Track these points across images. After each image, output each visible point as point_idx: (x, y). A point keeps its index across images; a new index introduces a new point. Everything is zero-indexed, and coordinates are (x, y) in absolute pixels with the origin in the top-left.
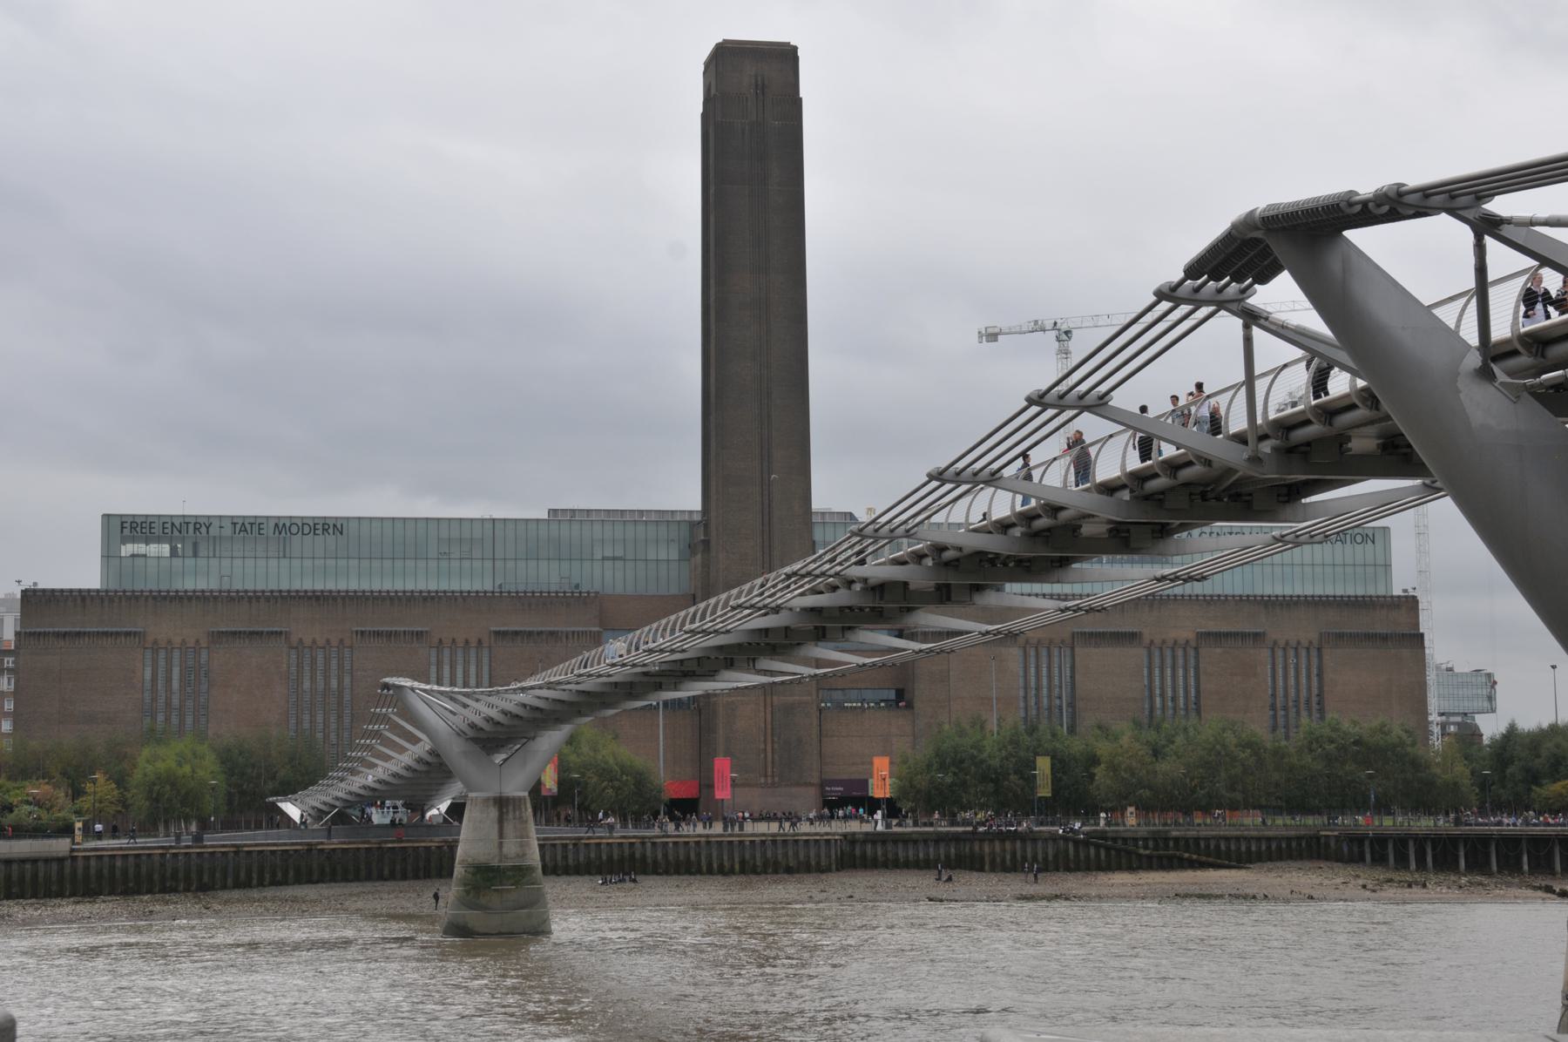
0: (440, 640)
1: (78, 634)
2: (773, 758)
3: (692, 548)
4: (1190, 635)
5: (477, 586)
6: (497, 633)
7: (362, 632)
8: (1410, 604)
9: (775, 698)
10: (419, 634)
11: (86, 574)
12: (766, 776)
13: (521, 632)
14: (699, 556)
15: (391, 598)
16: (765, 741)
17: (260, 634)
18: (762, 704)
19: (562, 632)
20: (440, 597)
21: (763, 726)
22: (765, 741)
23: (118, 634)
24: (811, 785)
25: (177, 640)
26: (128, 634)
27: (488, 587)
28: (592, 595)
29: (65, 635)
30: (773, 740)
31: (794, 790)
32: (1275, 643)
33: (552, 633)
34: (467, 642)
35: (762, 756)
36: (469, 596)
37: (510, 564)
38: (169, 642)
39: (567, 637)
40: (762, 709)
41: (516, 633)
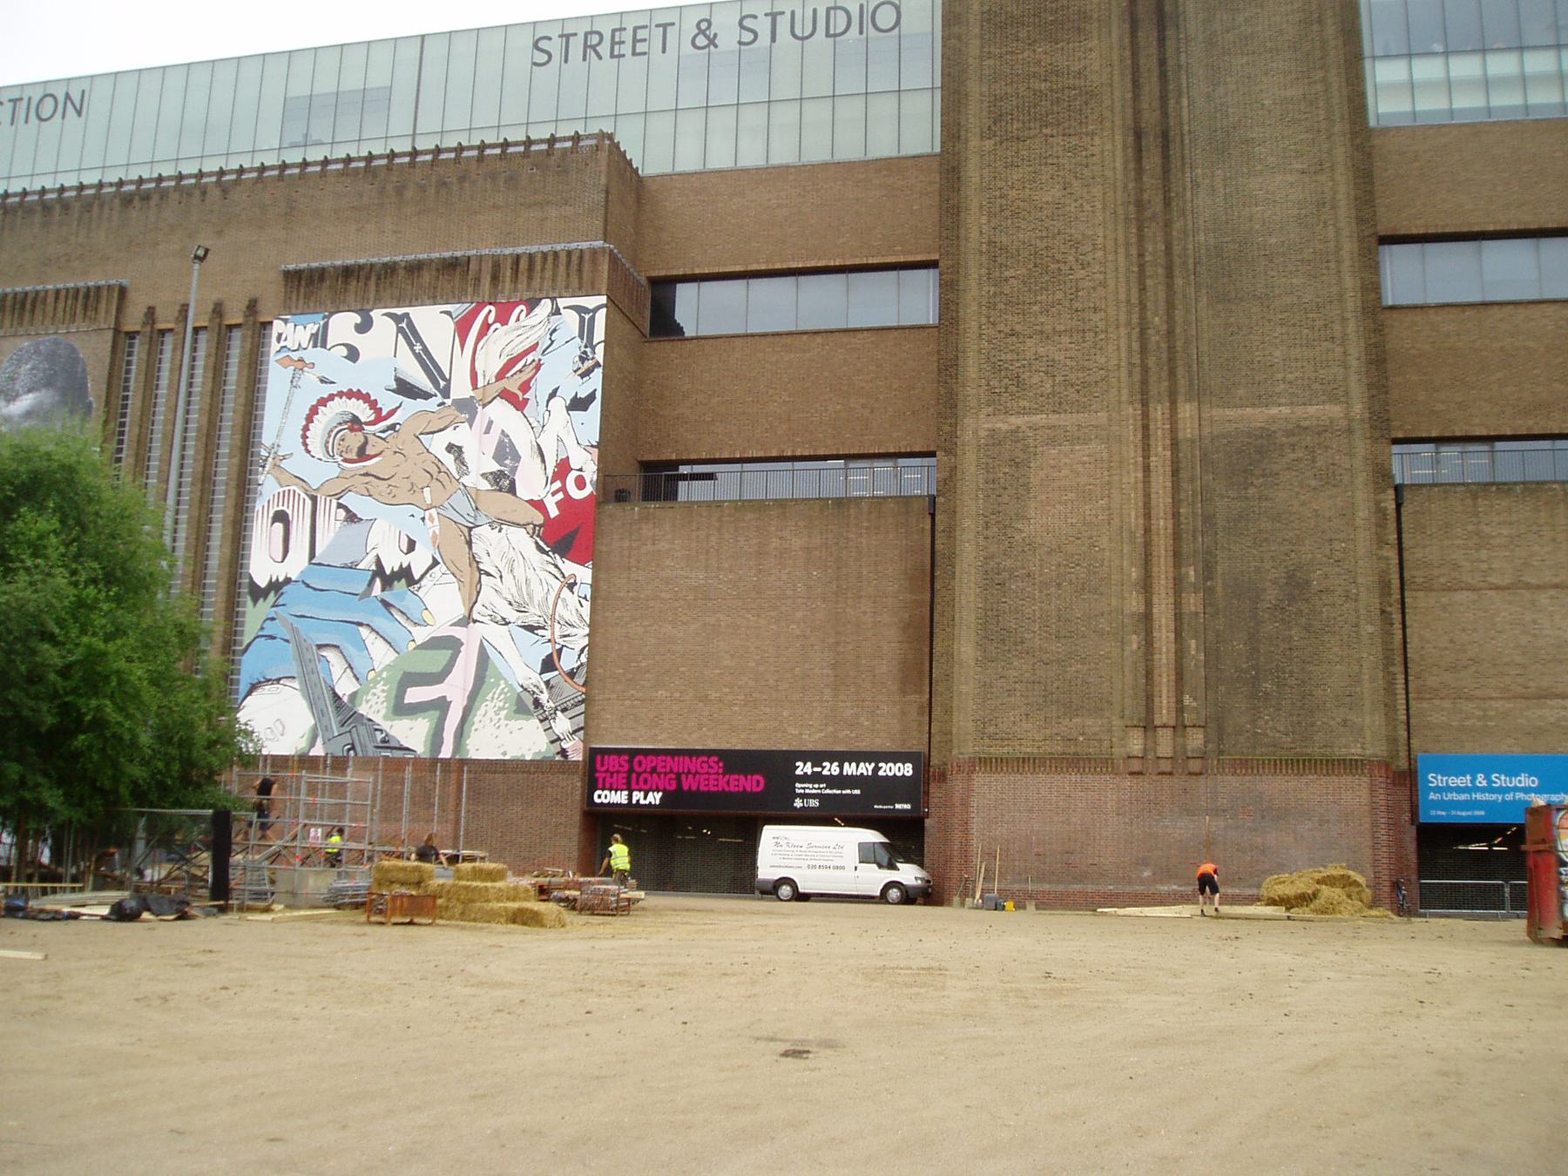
0: (151, 313)
2: (1180, 653)
9: (1186, 410)
12: (1148, 727)
13: (361, 267)
15: (46, 207)
16: (1146, 586)
18: (1132, 434)
19: (480, 258)
20: (164, 194)
21: (1134, 519)
22: (1146, 586)
24: (1352, 766)
30: (1178, 584)
31: (1277, 786)
33: (452, 266)
35: (1134, 642)
36: (237, 182)
39: (495, 278)
40: (1133, 454)
41: (348, 273)
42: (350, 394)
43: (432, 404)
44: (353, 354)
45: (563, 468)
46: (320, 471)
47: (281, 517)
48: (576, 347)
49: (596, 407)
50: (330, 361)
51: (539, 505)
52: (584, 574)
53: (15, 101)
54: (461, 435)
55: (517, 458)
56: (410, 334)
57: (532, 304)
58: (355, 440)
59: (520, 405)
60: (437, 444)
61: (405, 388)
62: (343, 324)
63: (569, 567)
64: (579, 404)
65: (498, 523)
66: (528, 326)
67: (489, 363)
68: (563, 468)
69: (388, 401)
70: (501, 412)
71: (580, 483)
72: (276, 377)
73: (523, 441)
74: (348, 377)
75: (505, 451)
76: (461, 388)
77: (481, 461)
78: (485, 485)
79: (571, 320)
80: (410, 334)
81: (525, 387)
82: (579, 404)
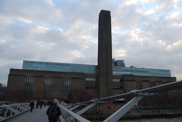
1: (17, 75)
3: (97, 69)
4: (154, 81)
5: (70, 72)
6: (72, 78)
10: (62, 77)
11: (20, 67)
14: (98, 69)
17: (40, 76)
23: (21, 75)
25: (30, 76)
26: (23, 75)
27: (71, 72)
29: (15, 75)
33: (79, 78)
37: (74, 69)
38: (29, 77)
41: (74, 78)
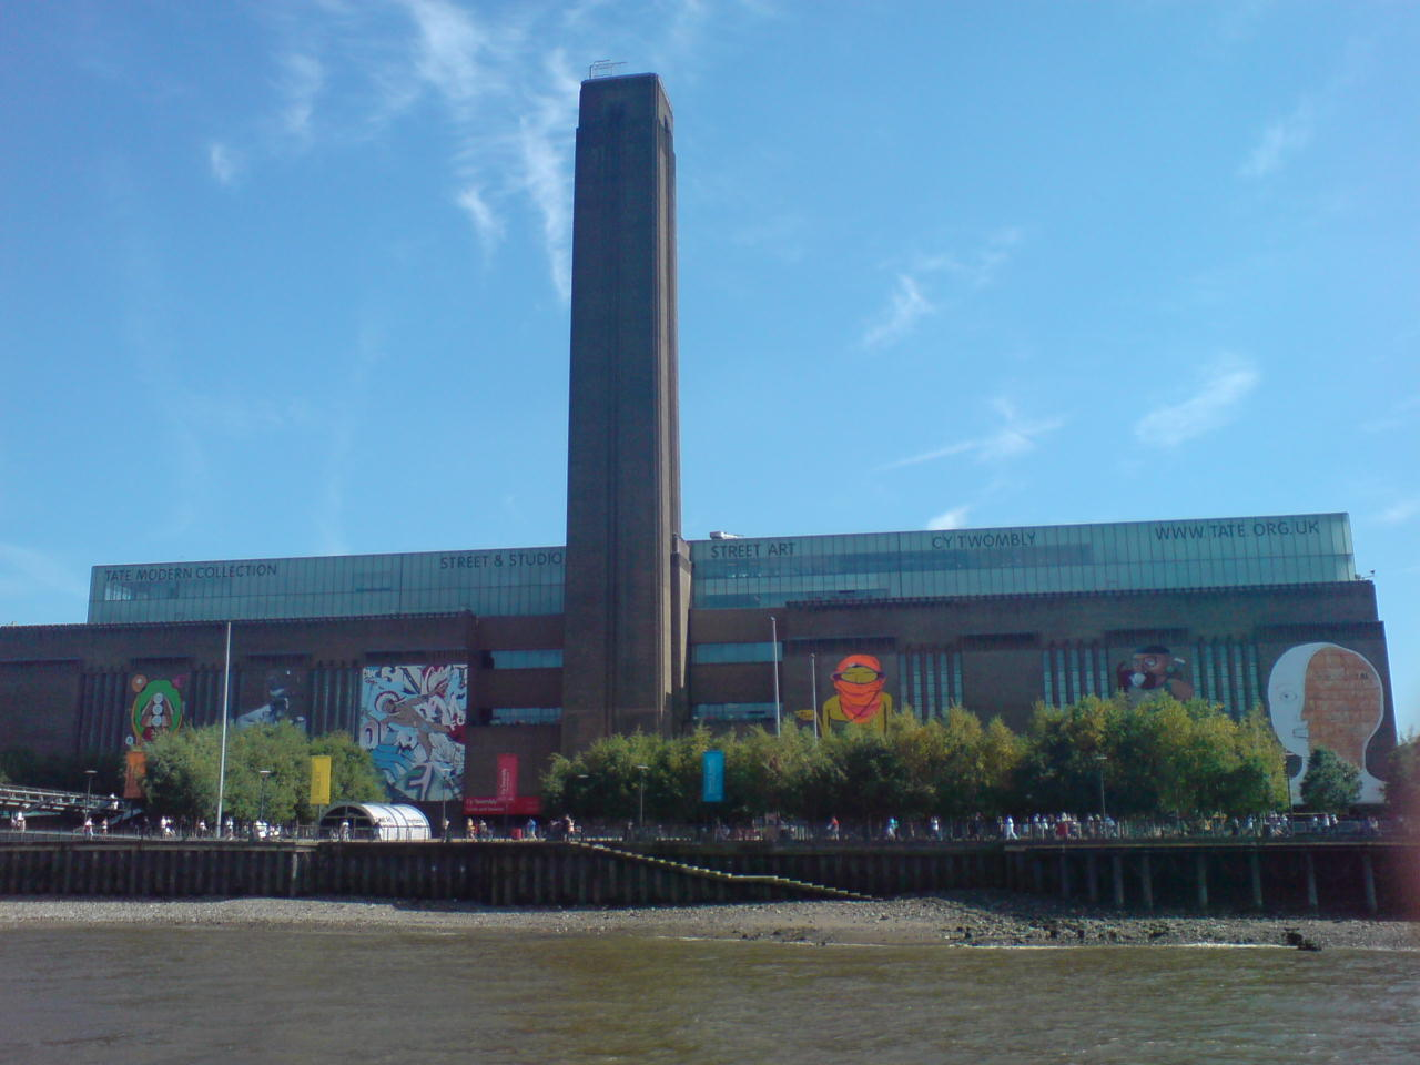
7: (252, 657)
8: (1365, 590)
23: (61, 662)
28: (453, 616)
32: (1201, 639)
34: (343, 663)
41: (387, 654)
42: (390, 692)
43: (415, 696)
44: (390, 680)
45: (455, 716)
46: (381, 716)
47: (369, 730)
48: (458, 680)
49: (465, 698)
50: (382, 682)
51: (449, 727)
52: (462, 747)
53: (248, 567)
54: (425, 706)
55: (441, 712)
56: (407, 673)
57: (445, 667)
58: (391, 707)
59: (442, 696)
60: (417, 708)
61: (406, 691)
62: (386, 670)
63: (458, 745)
64: (460, 697)
65: (436, 732)
66: (444, 672)
67: (433, 684)
68: (455, 716)
69: (401, 695)
70: (436, 699)
71: (461, 720)
72: (365, 687)
73: (443, 707)
74: (389, 688)
75: (438, 711)
76: (424, 692)
77: (431, 714)
78: (432, 721)
79: (457, 672)
80: (407, 673)
81: (444, 691)
82: (460, 697)
